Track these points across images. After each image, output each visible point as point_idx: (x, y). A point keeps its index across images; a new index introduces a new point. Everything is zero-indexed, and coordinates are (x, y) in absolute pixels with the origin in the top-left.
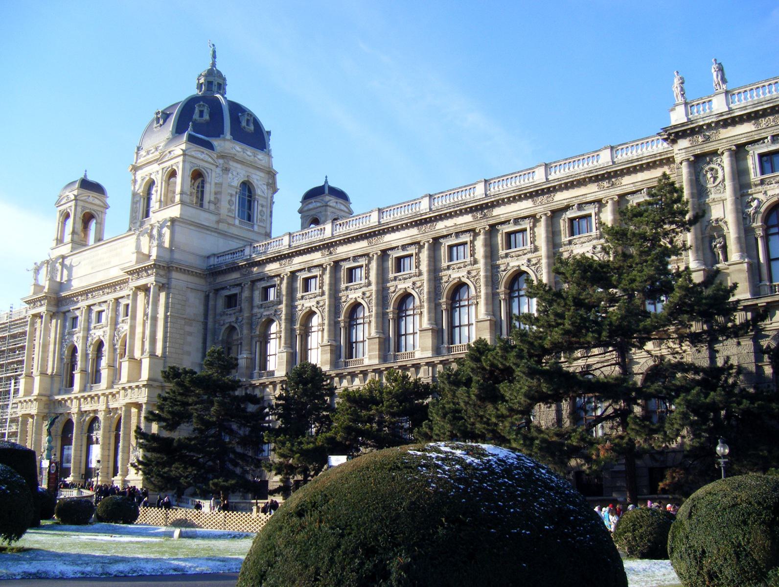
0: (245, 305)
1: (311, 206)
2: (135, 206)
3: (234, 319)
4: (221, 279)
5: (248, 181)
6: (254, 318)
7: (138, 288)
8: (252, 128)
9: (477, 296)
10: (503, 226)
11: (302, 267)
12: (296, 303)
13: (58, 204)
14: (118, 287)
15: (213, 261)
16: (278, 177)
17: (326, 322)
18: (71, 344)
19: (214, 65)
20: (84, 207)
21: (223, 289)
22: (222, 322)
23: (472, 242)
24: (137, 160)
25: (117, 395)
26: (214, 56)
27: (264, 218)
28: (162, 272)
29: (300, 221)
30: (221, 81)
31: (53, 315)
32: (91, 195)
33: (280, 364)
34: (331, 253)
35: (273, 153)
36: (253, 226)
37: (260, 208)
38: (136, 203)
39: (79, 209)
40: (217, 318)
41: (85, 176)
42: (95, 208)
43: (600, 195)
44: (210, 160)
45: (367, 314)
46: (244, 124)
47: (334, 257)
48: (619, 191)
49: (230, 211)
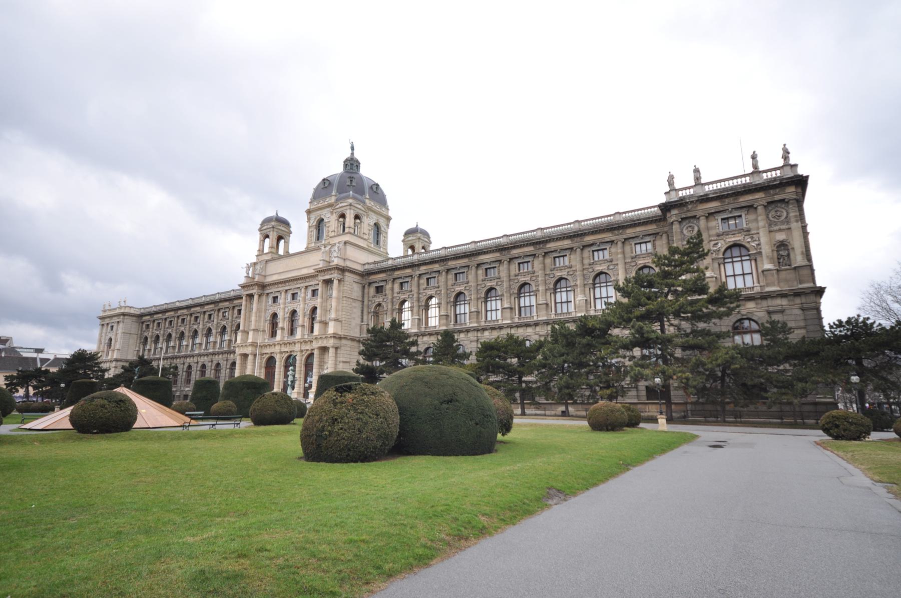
0: (388, 292)
1: (410, 239)
3: (381, 300)
15: (367, 267)
16: (391, 221)
19: (352, 154)
21: (374, 282)
22: (373, 302)
23: (533, 261)
26: (353, 149)
28: (340, 272)
30: (358, 164)
35: (389, 208)
36: (380, 247)
38: (311, 232)
39: (275, 234)
41: (277, 214)
42: (284, 233)
43: (613, 238)
44: (363, 209)
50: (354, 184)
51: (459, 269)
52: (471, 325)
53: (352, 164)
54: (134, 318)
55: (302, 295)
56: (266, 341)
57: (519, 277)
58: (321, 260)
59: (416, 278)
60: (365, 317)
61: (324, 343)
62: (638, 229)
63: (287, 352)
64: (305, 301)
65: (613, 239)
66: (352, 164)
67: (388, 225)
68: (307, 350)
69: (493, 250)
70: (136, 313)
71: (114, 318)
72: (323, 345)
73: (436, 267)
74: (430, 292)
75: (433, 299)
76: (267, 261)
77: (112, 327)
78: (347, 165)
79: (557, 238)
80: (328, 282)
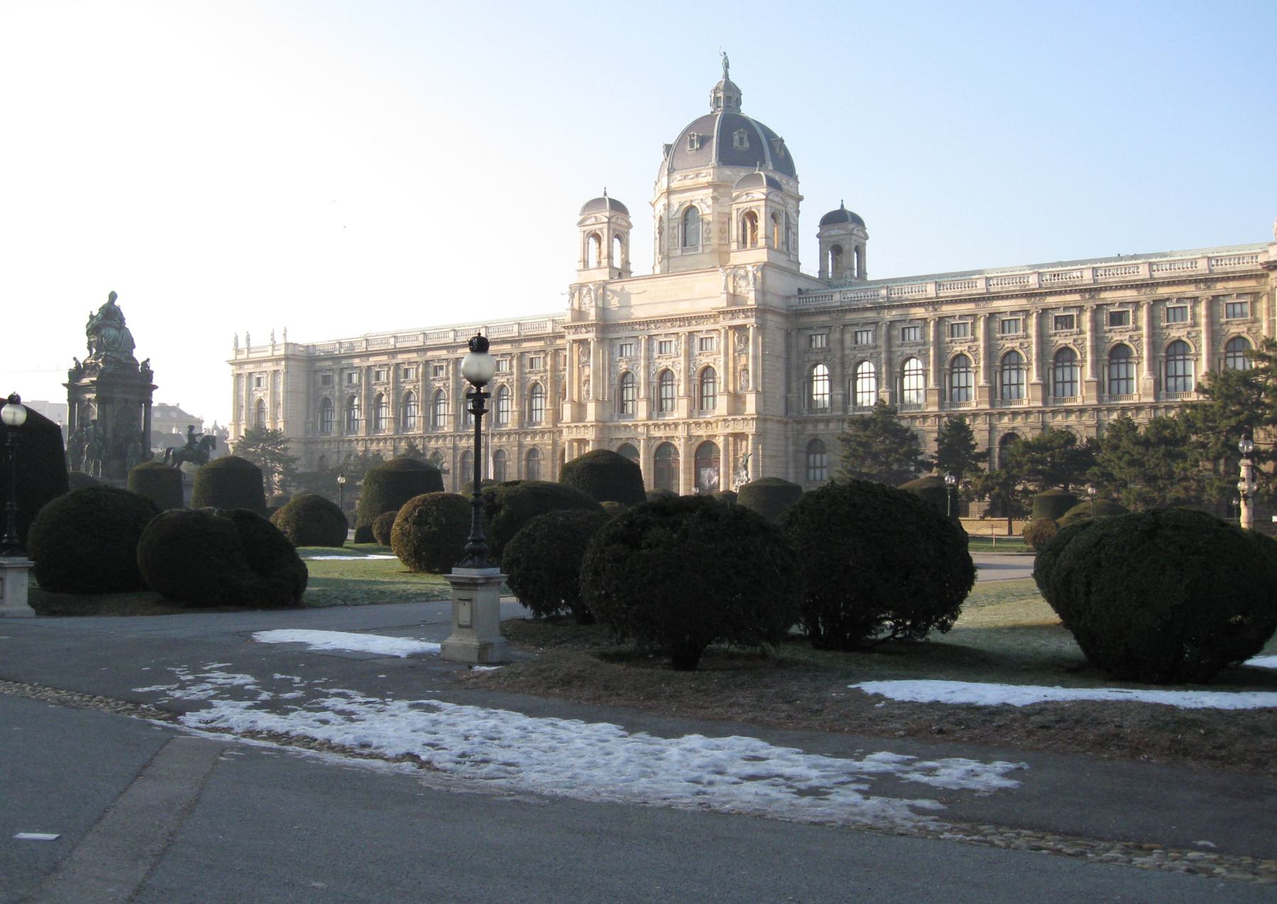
1: (833, 233)
2: (671, 231)
4: (805, 320)
6: (846, 358)
8: (783, 153)
9: (1083, 360)
10: (1109, 307)
11: (903, 318)
12: (894, 349)
13: (581, 223)
15: (794, 302)
17: (931, 368)
19: (726, 76)
20: (614, 230)
21: (807, 329)
25: (714, 425)
26: (727, 66)
31: (601, 341)
34: (936, 310)
35: (799, 180)
38: (673, 228)
41: (605, 194)
43: (1197, 294)
44: (781, 202)
46: (778, 150)
47: (939, 313)
48: (1213, 293)
52: (980, 407)
53: (729, 95)
54: (301, 364)
56: (616, 418)
59: (884, 328)
60: (794, 385)
61: (739, 428)
62: (1231, 285)
63: (661, 438)
65: (1197, 295)
66: (729, 95)
67: (798, 212)
68: (699, 436)
69: (1017, 295)
70: (301, 354)
71: (264, 364)
72: (736, 431)
74: (908, 351)
75: (913, 361)
77: (259, 379)
79: (1116, 287)
80: (741, 329)
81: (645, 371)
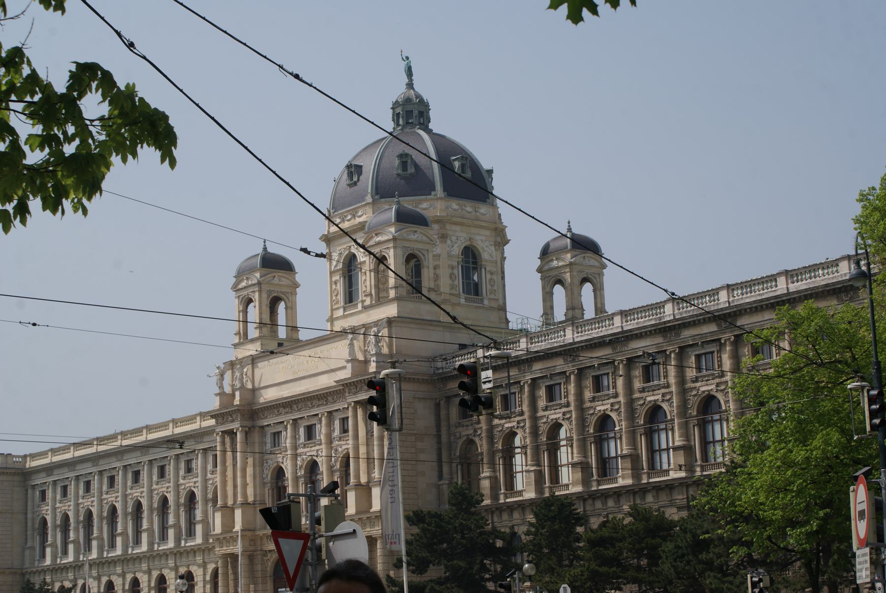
2: (334, 287)
3: (471, 432)
5: (471, 245)
7: (355, 402)
14: (330, 398)
18: (275, 465)
19: (410, 85)
20: (269, 292)
23: (719, 351)
24: (329, 228)
26: (409, 72)
27: (495, 288)
29: (540, 282)
30: (422, 109)
32: (276, 274)
33: (528, 484)
36: (482, 300)
37: (489, 276)
38: (336, 283)
39: (265, 295)
40: (452, 429)
41: (265, 249)
42: (284, 290)
45: (617, 428)
49: (452, 287)
50: (411, 170)
51: (599, 368)
54: (16, 478)
55: (324, 431)
57: (698, 384)
58: (348, 361)
59: (526, 389)
60: (445, 469)
64: (331, 443)
69: (650, 331)
73: (559, 364)
74: (555, 415)
76: (254, 360)
78: (398, 114)
79: (751, 309)
81: (292, 466)
